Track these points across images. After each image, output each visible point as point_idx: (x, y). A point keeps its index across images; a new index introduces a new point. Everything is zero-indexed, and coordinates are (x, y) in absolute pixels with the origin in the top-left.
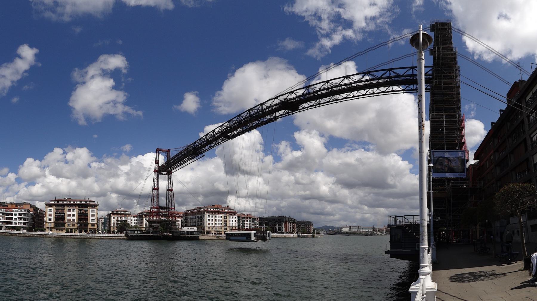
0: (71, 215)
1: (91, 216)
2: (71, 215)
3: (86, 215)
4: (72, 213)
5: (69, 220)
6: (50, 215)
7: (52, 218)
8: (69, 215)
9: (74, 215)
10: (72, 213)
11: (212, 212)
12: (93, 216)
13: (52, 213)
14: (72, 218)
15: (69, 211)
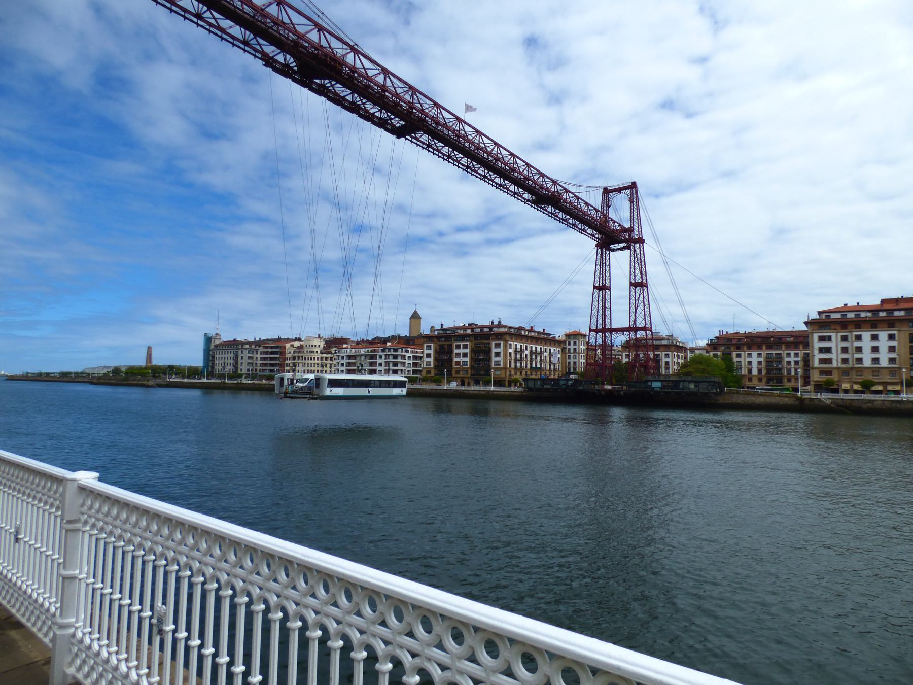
0: (462, 355)
1: (493, 354)
2: (462, 355)
3: (488, 352)
4: (462, 351)
5: (458, 363)
6: (429, 356)
7: (431, 360)
8: (458, 355)
9: (465, 355)
10: (462, 351)
11: (844, 324)
12: (498, 354)
13: (431, 352)
14: (461, 359)
15: (458, 347)
